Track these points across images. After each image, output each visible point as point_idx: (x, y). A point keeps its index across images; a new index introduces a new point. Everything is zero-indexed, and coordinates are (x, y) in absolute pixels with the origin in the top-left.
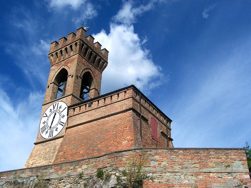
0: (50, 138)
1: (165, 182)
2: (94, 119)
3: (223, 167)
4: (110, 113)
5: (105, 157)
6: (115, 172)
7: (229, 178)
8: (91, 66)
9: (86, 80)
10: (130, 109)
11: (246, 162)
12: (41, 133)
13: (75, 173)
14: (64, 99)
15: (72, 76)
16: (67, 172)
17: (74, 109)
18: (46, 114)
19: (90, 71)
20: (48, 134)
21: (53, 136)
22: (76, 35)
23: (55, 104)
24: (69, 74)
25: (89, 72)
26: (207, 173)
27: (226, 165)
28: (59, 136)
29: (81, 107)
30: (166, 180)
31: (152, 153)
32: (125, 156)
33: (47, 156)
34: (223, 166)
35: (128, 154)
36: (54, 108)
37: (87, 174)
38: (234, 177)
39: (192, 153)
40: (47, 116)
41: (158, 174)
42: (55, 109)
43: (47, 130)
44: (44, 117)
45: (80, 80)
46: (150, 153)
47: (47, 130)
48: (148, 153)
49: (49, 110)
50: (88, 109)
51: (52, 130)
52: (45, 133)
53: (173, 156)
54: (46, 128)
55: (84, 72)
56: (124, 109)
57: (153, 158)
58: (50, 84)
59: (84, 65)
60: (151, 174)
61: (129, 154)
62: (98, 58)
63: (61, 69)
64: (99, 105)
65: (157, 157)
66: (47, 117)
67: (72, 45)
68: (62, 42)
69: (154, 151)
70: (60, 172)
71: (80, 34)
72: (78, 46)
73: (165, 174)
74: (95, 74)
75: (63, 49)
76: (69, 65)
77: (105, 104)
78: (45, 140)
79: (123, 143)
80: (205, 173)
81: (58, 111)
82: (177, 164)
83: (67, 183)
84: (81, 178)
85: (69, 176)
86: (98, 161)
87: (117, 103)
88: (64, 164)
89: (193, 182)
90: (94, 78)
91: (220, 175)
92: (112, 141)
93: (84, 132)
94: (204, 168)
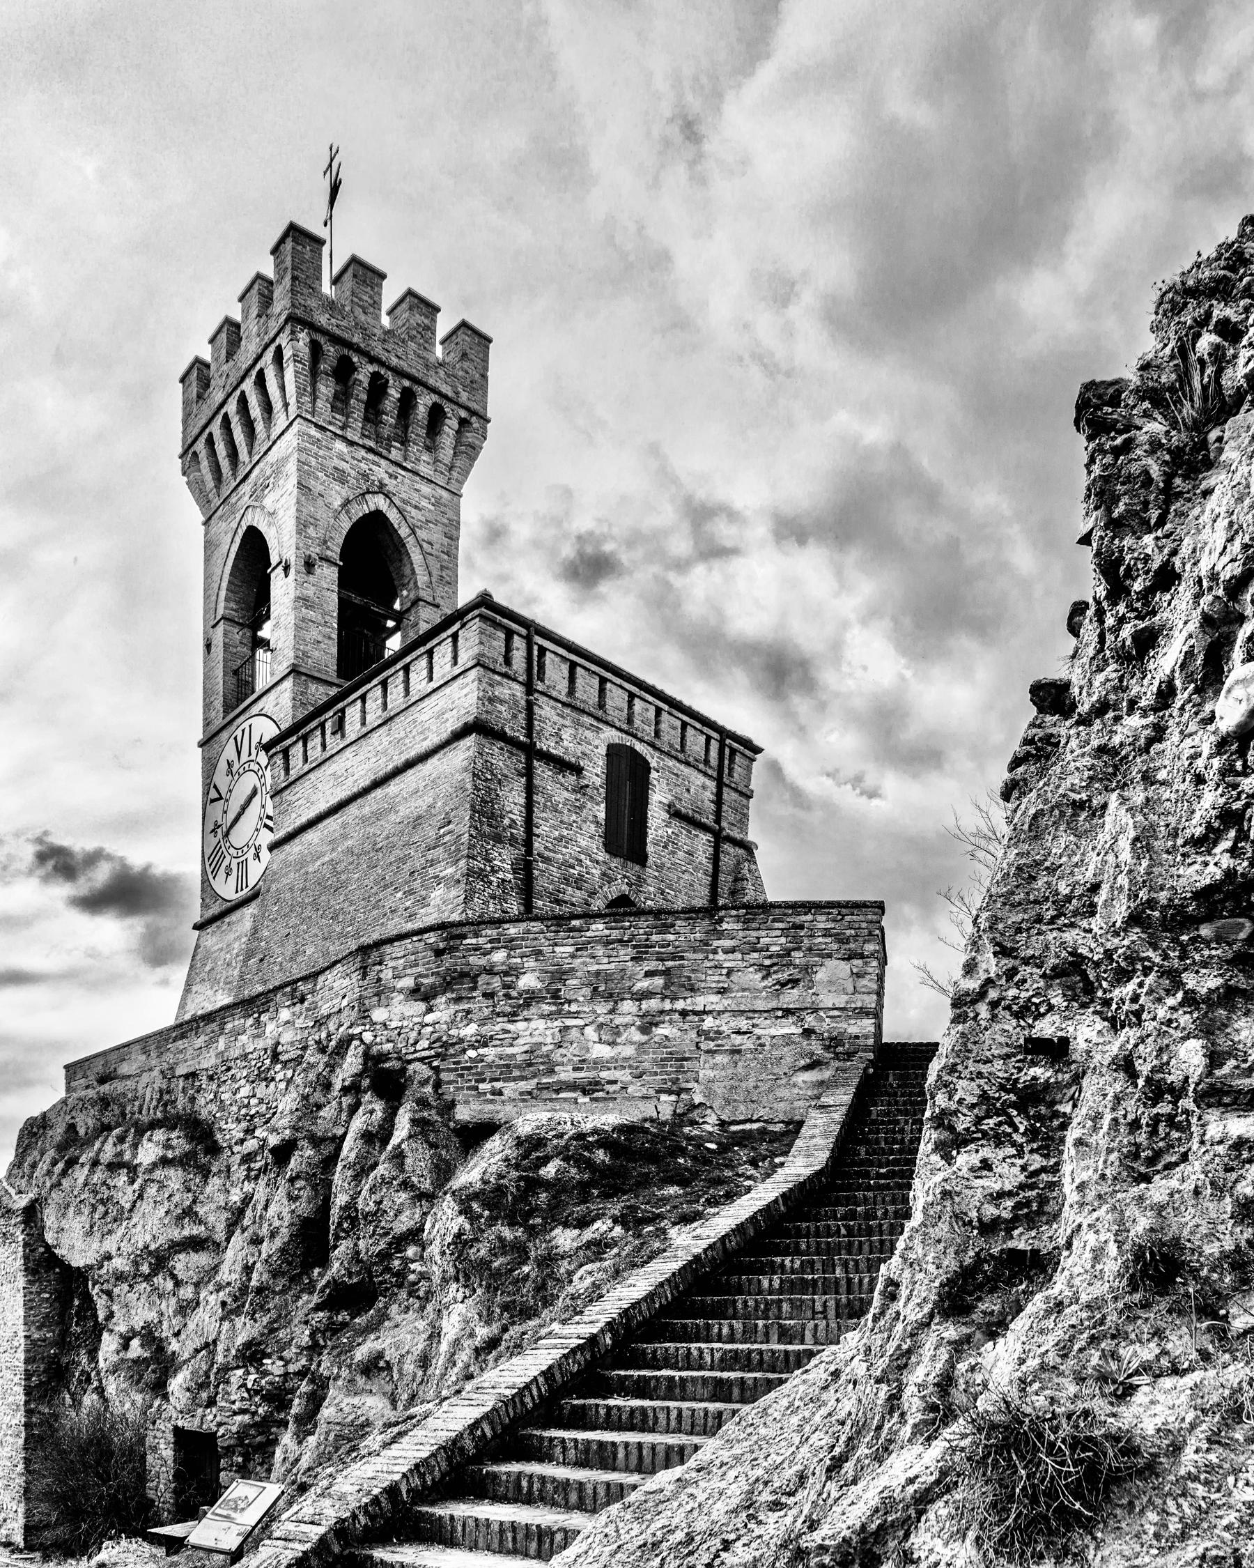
1: (526, 1056)
8: (381, 471)
9: (371, 563)
13: (261, 1044)
15: (286, 569)
25: (378, 515)
30: (526, 1048)
31: (481, 940)
32: (391, 964)
37: (292, 1043)
41: (498, 1028)
45: (328, 575)
46: (474, 941)
50: (334, 743)
55: (346, 525)
59: (341, 477)
69: (489, 932)
74: (414, 512)
76: (268, 502)
90: (410, 543)
92: (399, 895)
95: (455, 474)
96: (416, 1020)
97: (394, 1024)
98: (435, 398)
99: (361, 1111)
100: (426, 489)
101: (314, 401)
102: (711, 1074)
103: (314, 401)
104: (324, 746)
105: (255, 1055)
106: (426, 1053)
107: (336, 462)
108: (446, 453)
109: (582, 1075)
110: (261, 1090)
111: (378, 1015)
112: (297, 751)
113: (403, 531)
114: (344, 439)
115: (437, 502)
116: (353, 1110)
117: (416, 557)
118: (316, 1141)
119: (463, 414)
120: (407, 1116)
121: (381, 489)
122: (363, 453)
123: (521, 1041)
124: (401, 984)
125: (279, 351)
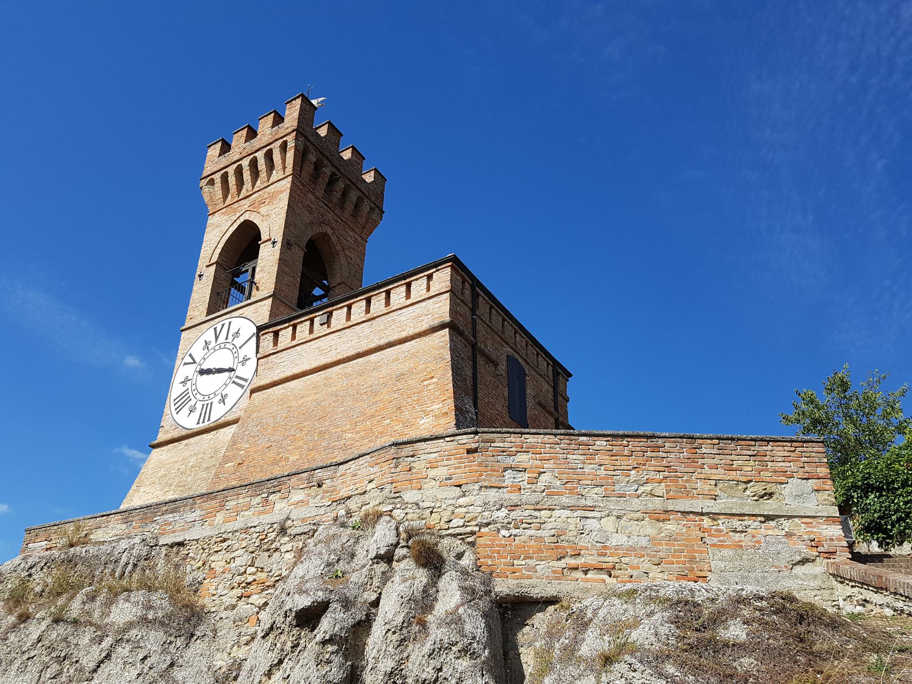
0: (201, 425)
1: (554, 539)
2: (335, 359)
3: (749, 496)
4: (383, 342)
5: (361, 461)
6: (390, 507)
7: (770, 532)
8: (330, 216)
10: (442, 326)
11: (830, 482)
12: (174, 412)
14: (247, 311)
16: (243, 516)
17: (276, 334)
18: (190, 355)
19: (330, 232)
20: (195, 416)
21: (212, 420)
22: (282, 120)
23: (219, 326)
24: (264, 237)
25: (326, 234)
26: (691, 516)
27: (759, 488)
28: (230, 418)
29: (299, 328)
30: (552, 532)
32: (423, 457)
33: (189, 479)
34: (748, 492)
35: (432, 451)
36: (217, 338)
37: (303, 520)
38: (787, 530)
39: (638, 449)
40: (195, 362)
41: (527, 513)
42: (219, 341)
43: (192, 403)
44: (185, 364)
45: (299, 254)
47: (192, 403)
48: (496, 444)
49: (201, 343)
51: (209, 402)
52: (186, 410)
53: (574, 457)
54: (192, 397)
56: (425, 326)
57: (509, 461)
58: (207, 266)
60: (504, 512)
61: (436, 450)
62: (354, 195)
63: (239, 222)
64: (352, 317)
65: (522, 459)
66: (195, 365)
67: (271, 150)
68: (243, 139)
70: (220, 517)
71: (296, 114)
72: (290, 155)
73: (549, 512)
74: (344, 241)
75: (245, 163)
77: (369, 316)
78: (184, 433)
79: (421, 422)
80: (684, 513)
81: (228, 346)
82: (589, 482)
83: (240, 552)
84: (283, 531)
85: (246, 530)
86: (339, 474)
87: (404, 310)
88: (231, 492)
89: (644, 542)
91: (736, 523)
92: (388, 421)
93: (305, 399)
94: (681, 498)
95: (365, 230)
96: (453, 502)
97: (426, 505)
98: (360, 194)
99: (397, 578)
100: (351, 234)
101: (301, 171)
102: (722, 565)
103: (301, 171)
104: (311, 331)
105: (258, 529)
106: (462, 530)
107: (308, 202)
108: (362, 221)
109: (606, 559)
110: (262, 559)
111: (410, 496)
112: (286, 335)
113: (339, 248)
114: (314, 194)
115: (356, 241)
116: (386, 578)
117: (344, 262)
118: (347, 604)
119: (373, 206)
120: (455, 585)
121: (328, 224)
122: (322, 204)
123: (549, 526)
124: (432, 473)
125: (285, 143)
